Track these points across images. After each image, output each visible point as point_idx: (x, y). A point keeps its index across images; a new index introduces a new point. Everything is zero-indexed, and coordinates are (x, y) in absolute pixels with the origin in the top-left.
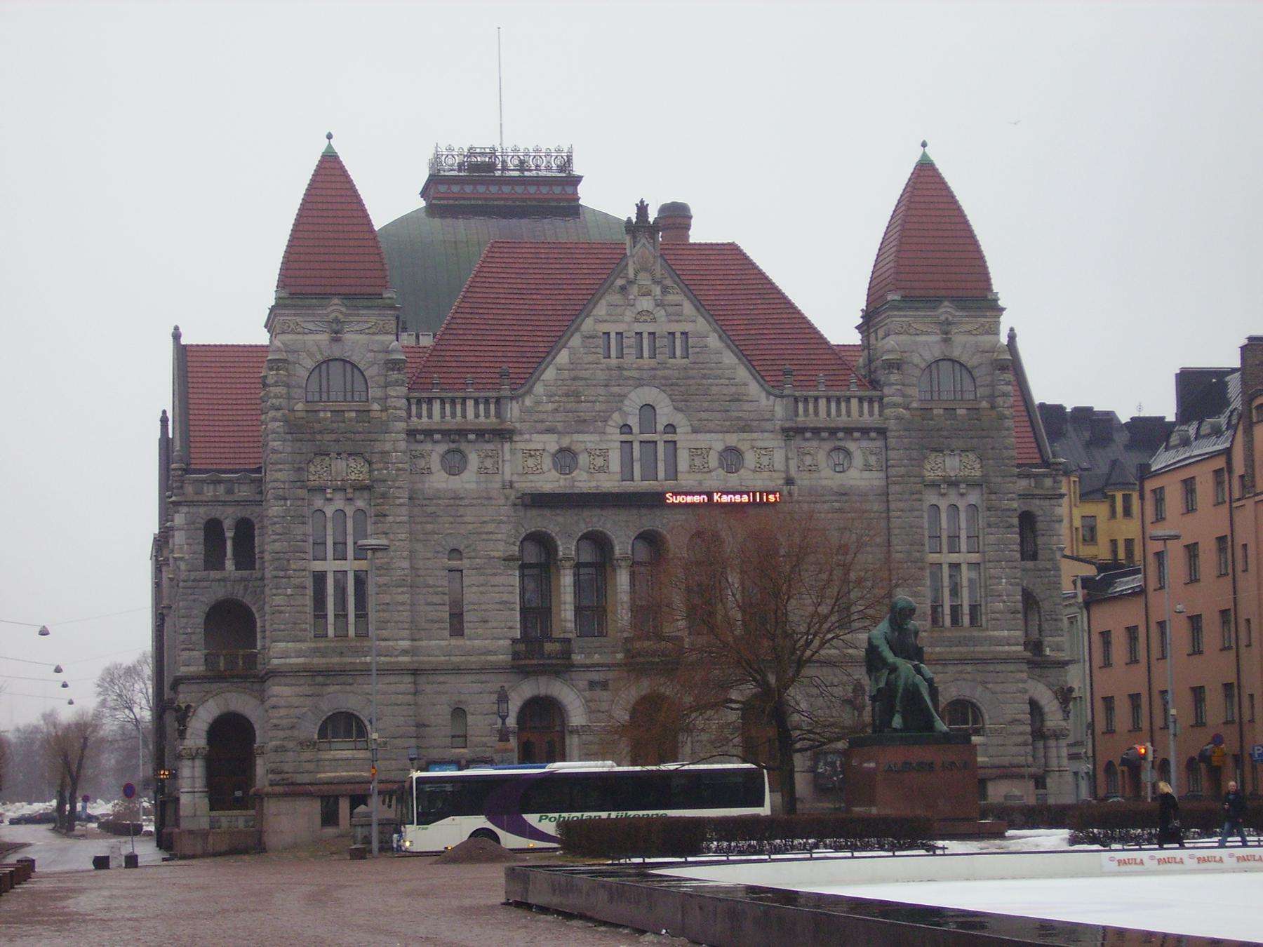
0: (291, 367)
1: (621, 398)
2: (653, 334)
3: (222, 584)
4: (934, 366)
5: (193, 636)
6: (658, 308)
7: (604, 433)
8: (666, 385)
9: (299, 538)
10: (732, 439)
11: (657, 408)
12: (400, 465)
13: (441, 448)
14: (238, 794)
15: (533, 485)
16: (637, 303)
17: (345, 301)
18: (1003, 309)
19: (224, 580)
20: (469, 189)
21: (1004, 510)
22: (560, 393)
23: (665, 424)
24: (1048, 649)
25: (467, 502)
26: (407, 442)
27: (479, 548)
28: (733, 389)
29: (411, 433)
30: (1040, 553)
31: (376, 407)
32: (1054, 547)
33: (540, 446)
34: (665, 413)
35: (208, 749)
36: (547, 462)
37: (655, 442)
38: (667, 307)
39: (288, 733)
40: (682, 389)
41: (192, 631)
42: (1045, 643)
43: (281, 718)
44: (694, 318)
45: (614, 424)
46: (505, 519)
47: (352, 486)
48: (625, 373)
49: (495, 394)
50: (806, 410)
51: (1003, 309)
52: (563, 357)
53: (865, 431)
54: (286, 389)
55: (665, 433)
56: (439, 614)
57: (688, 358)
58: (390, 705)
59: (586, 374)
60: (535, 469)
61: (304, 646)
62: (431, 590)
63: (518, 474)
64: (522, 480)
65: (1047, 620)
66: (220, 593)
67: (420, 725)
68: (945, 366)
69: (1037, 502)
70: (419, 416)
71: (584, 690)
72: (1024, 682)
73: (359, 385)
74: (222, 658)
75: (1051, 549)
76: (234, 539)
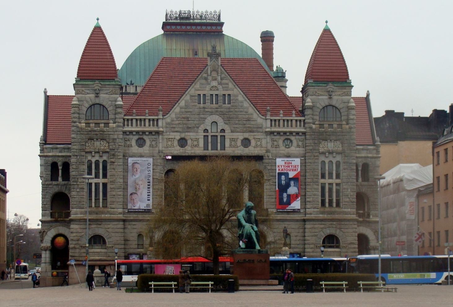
0: (80, 107)
4: (325, 108)
6: (219, 85)
7: (197, 132)
8: (222, 114)
9: (82, 170)
10: (246, 135)
11: (218, 123)
12: (120, 144)
13: (136, 137)
14: (59, 264)
15: (170, 151)
16: (211, 83)
17: (101, 82)
18: (353, 86)
19: (57, 185)
20: (178, 27)
21: (350, 163)
22: (181, 117)
23: (221, 129)
26: (123, 135)
28: (247, 116)
29: (125, 133)
30: (370, 179)
31: (111, 121)
33: (173, 137)
35: (51, 247)
36: (176, 143)
37: (217, 136)
39: (76, 242)
40: (228, 116)
42: (371, 213)
43: (74, 236)
46: (159, 164)
47: (102, 151)
49: (156, 117)
50: (275, 124)
51: (353, 86)
52: (182, 103)
53: (297, 133)
55: (221, 132)
57: (230, 104)
59: (191, 110)
61: (83, 210)
63: (165, 147)
66: (56, 189)
67: (126, 240)
68: (330, 108)
69: (369, 159)
70: (128, 125)
72: (356, 228)
73: (105, 114)
74: (57, 213)
76: (62, 169)
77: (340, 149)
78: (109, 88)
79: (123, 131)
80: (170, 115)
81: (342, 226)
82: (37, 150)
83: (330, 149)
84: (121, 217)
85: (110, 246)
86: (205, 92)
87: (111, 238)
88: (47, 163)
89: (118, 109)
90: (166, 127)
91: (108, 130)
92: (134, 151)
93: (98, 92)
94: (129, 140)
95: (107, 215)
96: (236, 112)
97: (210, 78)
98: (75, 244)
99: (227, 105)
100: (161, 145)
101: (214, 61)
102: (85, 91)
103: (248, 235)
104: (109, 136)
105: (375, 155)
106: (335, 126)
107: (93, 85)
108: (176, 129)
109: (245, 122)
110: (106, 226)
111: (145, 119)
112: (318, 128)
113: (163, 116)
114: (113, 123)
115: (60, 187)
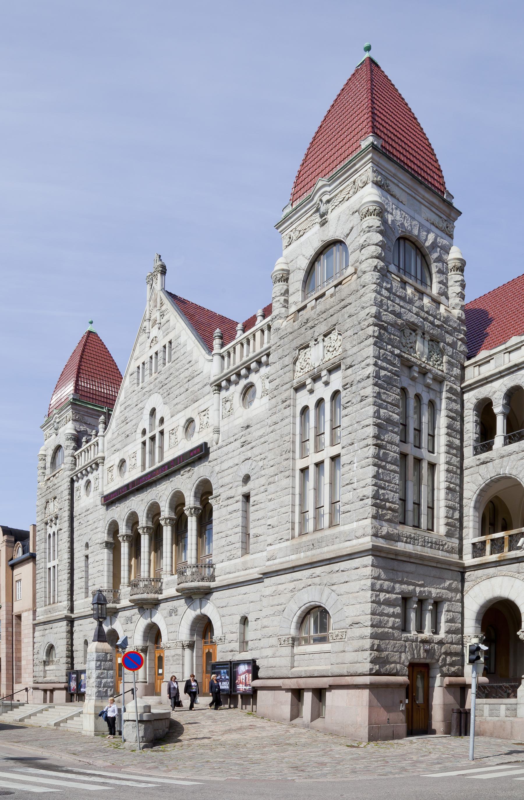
81: (336, 578)
108: (114, 448)
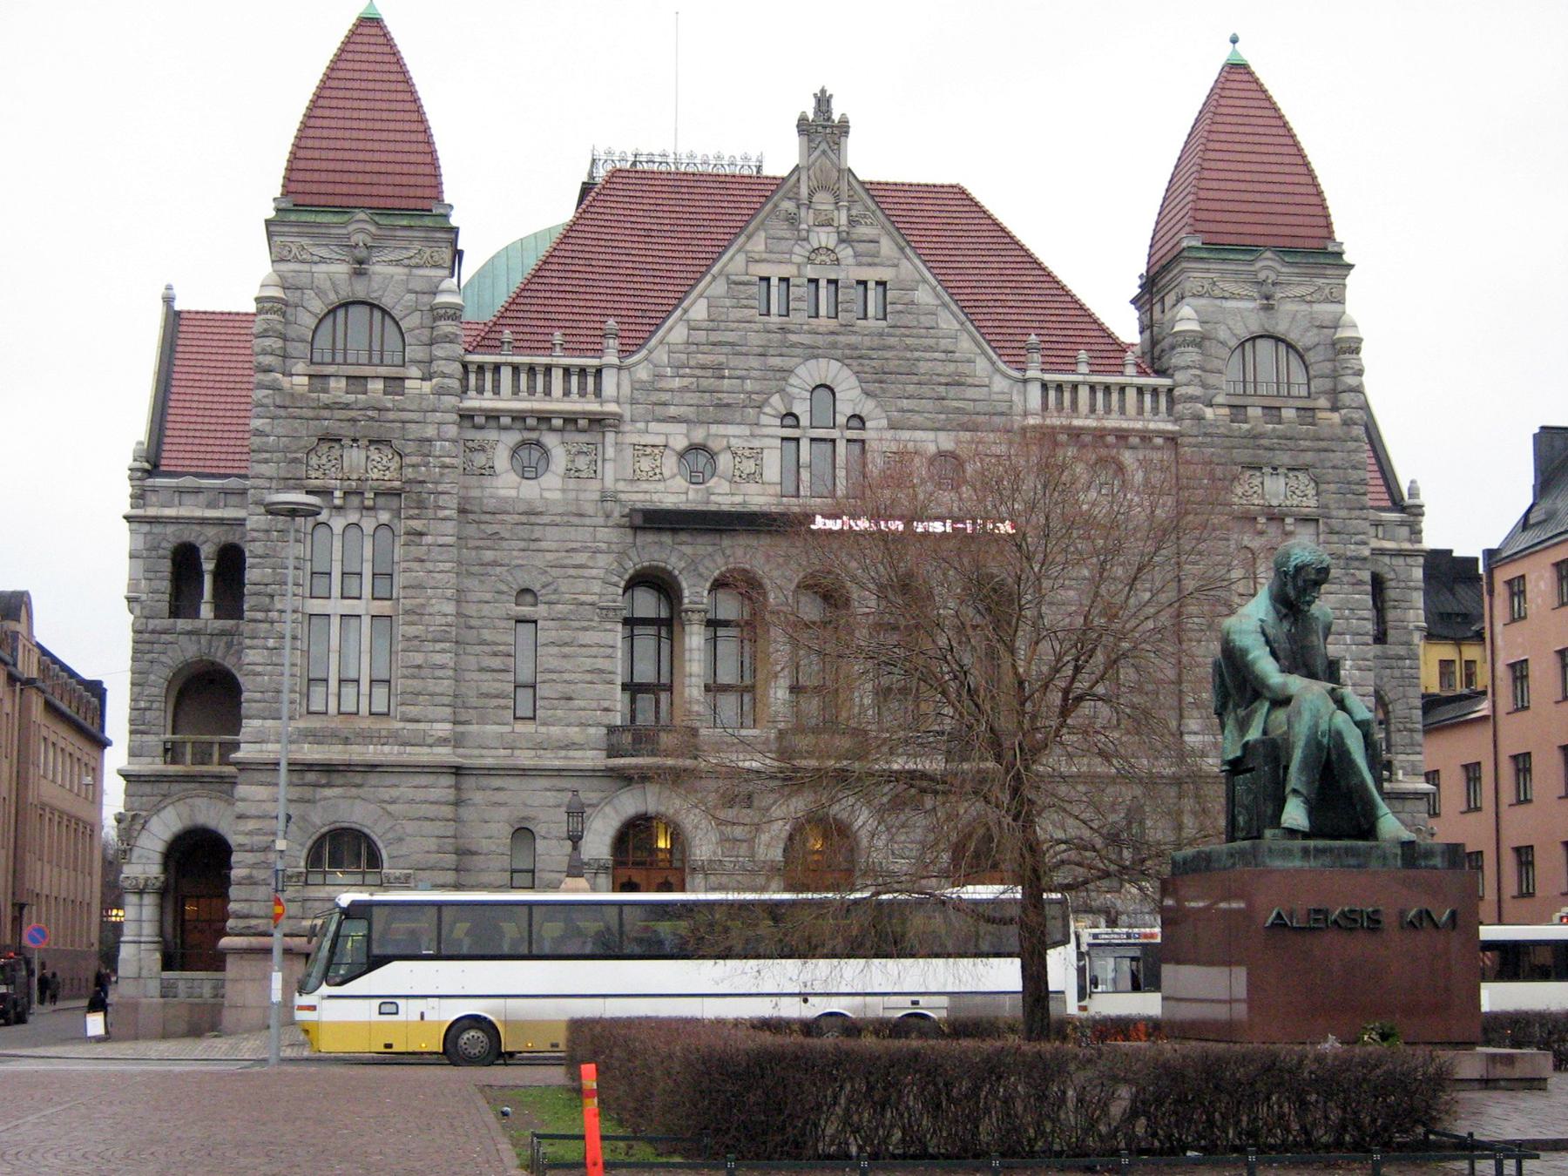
0: (290, 311)
1: (785, 374)
2: (835, 282)
3: (194, 638)
4: (1248, 346)
5: (147, 713)
8: (852, 357)
12: (447, 460)
13: (513, 438)
15: (648, 497)
17: (377, 218)
18: (1351, 266)
21: (1351, 558)
23: (849, 414)
24: (1400, 772)
25: (546, 519)
26: (460, 427)
27: (563, 589)
28: (951, 368)
29: (466, 417)
30: (1391, 632)
31: (414, 371)
32: (1411, 626)
33: (660, 440)
34: (850, 397)
35: (162, 878)
36: (670, 464)
37: (833, 441)
38: (855, 244)
39: (260, 857)
41: (148, 705)
42: (1396, 763)
43: (250, 833)
44: (896, 261)
45: (773, 412)
46: (604, 546)
48: (793, 338)
49: (596, 362)
50: (1060, 402)
51: (1351, 266)
52: (699, 310)
54: (280, 343)
55: (848, 428)
56: (497, 685)
57: (885, 318)
58: (418, 819)
60: (651, 474)
62: (486, 648)
64: (629, 489)
65: (1400, 731)
66: (189, 650)
68: (1265, 346)
69: (1387, 559)
70: (480, 390)
71: (715, 807)
75: (1406, 628)
76: (217, 575)
77: (1310, 504)
78: (410, 240)
79: (460, 409)
80: (650, 352)
82: (119, 495)
83: (1275, 503)
84: (444, 754)
85: (398, 872)
86: (787, 271)
87: (401, 840)
88: (155, 548)
89: (443, 322)
90: (633, 402)
91: (400, 407)
92: (502, 492)
93: (361, 253)
94: (483, 450)
95: (386, 749)
96: (908, 348)
97: (807, 217)
98: (254, 866)
99: (871, 323)
100: (609, 466)
101: (824, 152)
102: (314, 250)
103: (1319, 744)
104: (403, 429)
105: (1407, 546)
106: (1289, 414)
107: (344, 225)
108: (672, 411)
109: (942, 389)
110: (386, 794)
111: (548, 369)
112: (1228, 419)
113: (625, 352)
114: (422, 379)
115: (204, 640)
